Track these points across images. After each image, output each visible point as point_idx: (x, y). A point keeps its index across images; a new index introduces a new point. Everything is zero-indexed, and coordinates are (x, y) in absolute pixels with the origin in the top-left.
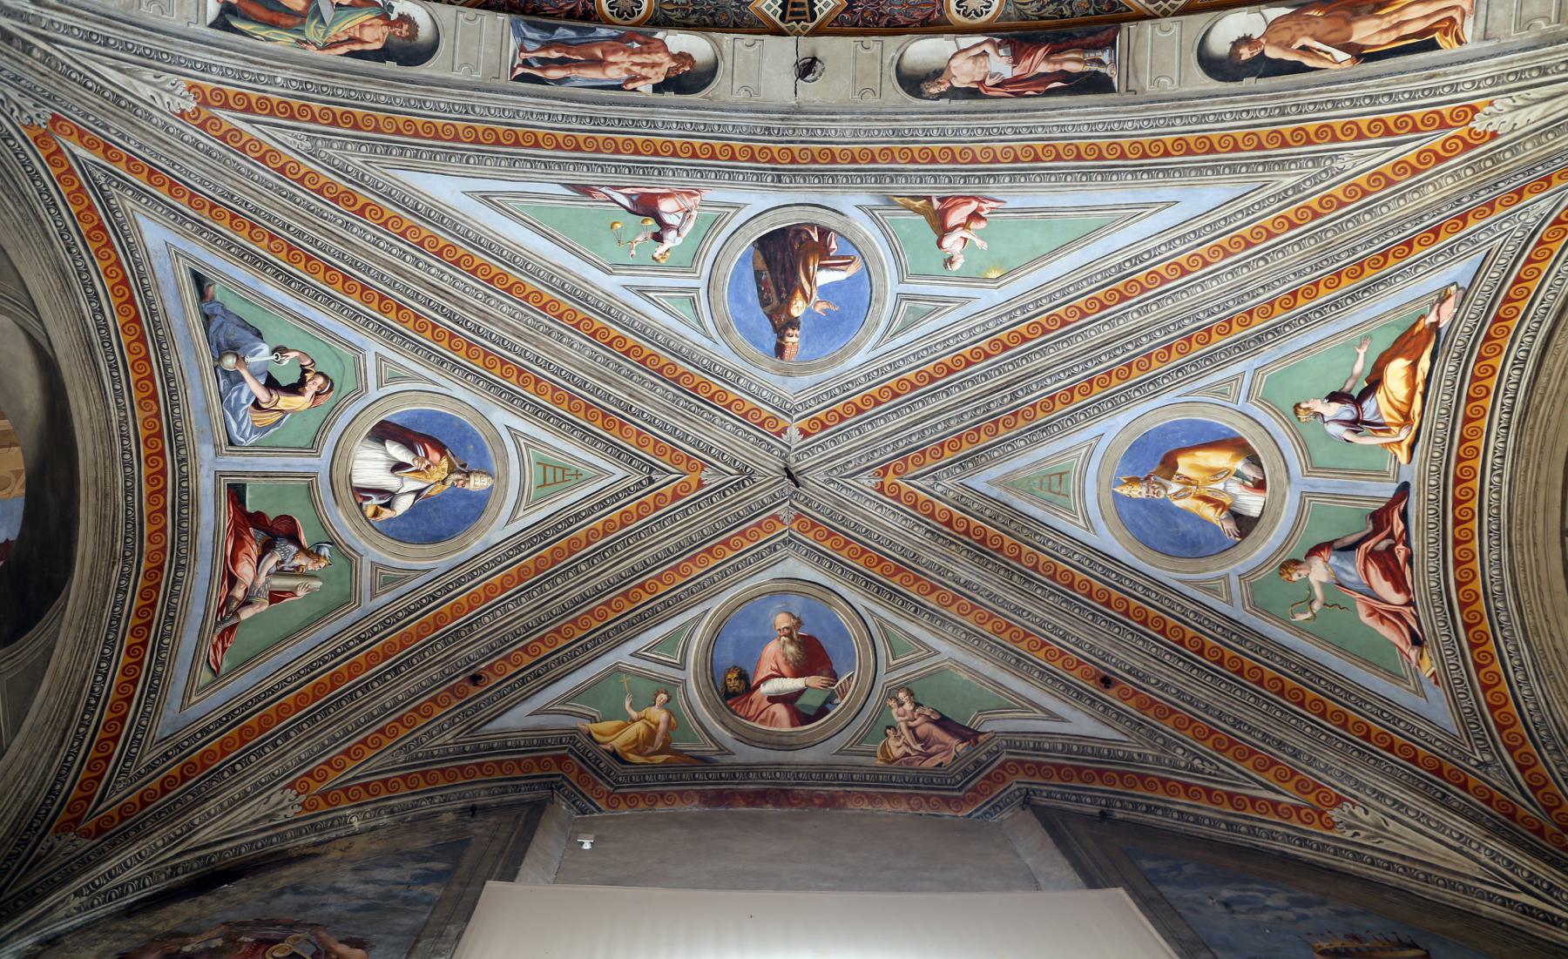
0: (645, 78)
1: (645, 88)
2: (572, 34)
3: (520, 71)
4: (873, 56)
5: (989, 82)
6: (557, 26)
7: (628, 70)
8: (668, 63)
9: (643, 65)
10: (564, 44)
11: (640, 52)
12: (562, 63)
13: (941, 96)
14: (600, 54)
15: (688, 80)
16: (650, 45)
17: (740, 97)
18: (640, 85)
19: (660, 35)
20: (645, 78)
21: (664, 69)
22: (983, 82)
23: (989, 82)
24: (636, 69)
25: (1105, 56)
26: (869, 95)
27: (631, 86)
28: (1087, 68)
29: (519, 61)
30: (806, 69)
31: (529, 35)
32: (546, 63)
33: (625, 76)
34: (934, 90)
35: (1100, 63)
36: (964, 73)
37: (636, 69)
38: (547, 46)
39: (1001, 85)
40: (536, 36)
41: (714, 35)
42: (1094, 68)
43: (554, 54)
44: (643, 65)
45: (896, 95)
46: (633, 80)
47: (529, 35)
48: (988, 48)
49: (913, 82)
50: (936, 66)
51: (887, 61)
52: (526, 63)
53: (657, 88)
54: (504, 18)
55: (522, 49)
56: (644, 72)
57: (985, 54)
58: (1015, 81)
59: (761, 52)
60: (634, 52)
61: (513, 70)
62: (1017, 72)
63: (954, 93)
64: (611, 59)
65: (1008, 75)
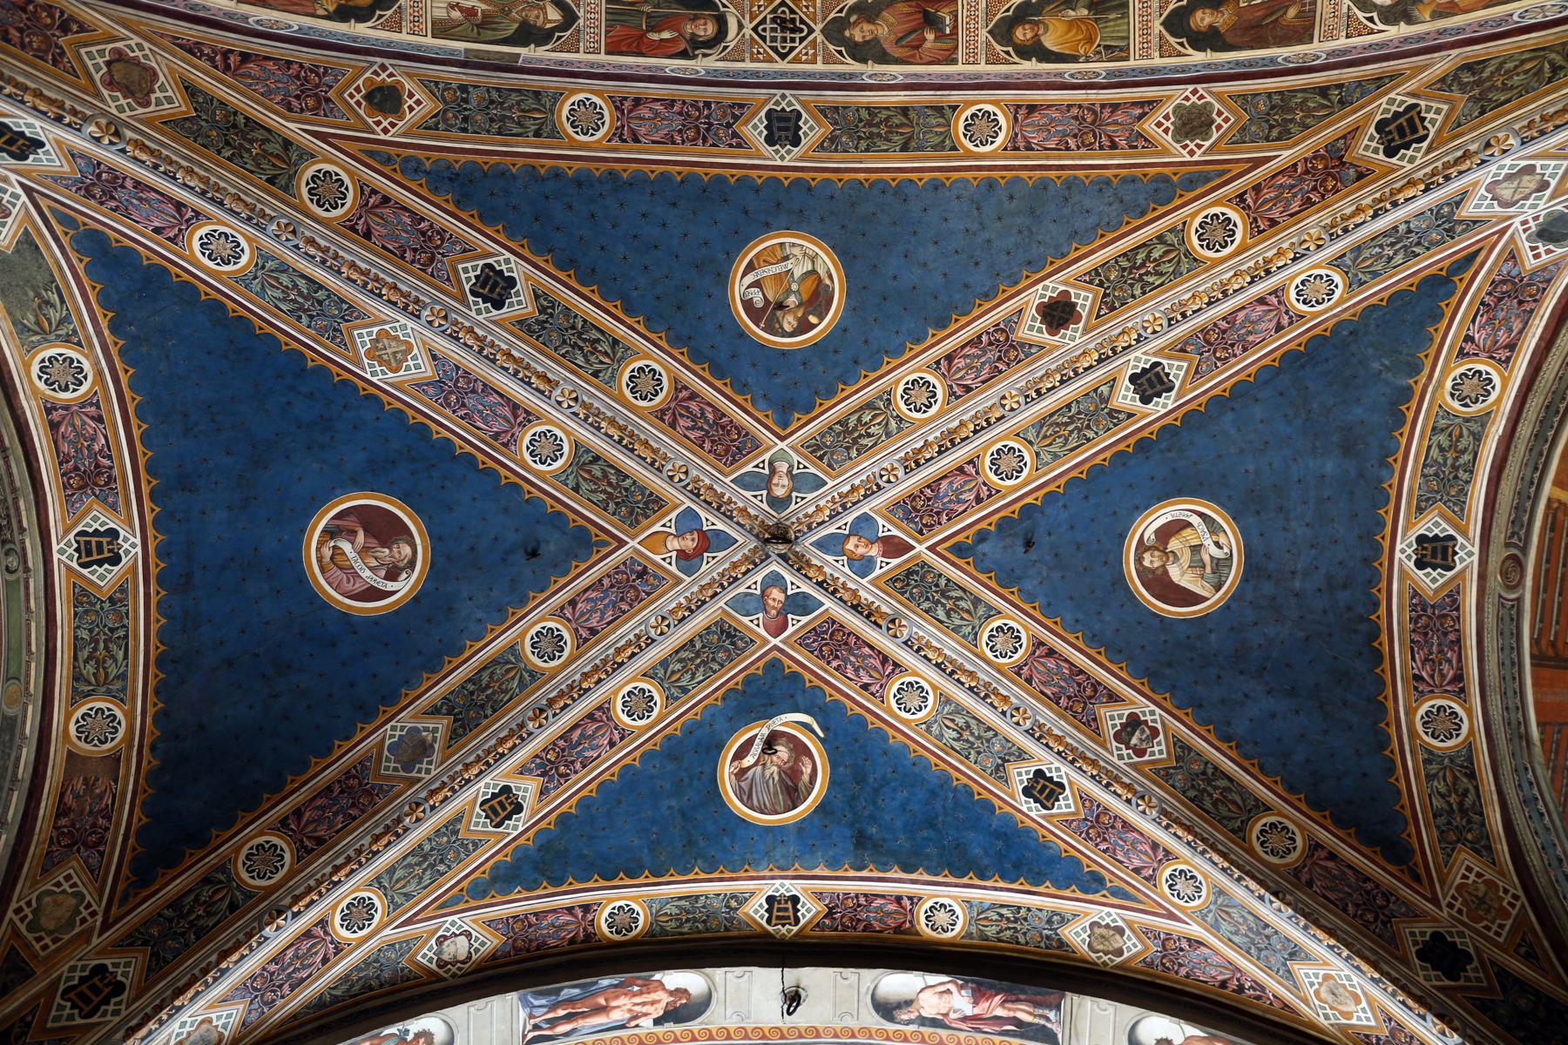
0: (646, 1015)
1: (647, 1023)
2: (577, 991)
3: (530, 1035)
4: (850, 986)
5: (952, 1016)
6: (562, 989)
7: (630, 1011)
8: (666, 999)
9: (644, 1004)
10: (570, 1001)
11: (641, 993)
12: (569, 1018)
13: (909, 1022)
14: (602, 1001)
15: (683, 1010)
16: (648, 987)
17: (732, 1023)
18: (643, 1022)
19: (658, 976)
20: (646, 1015)
21: (663, 1004)
22: (946, 1015)
23: (952, 1016)
24: (637, 1008)
25: (1052, 1015)
26: (848, 1017)
27: (633, 1023)
28: (1036, 1021)
29: (529, 1027)
30: (793, 999)
31: (536, 1003)
32: (553, 1022)
33: (628, 1016)
34: (905, 1017)
35: (1048, 1019)
36: (930, 1005)
37: (637, 1008)
38: (553, 1007)
39: (965, 1019)
40: (543, 1002)
41: (708, 970)
42: (1042, 1022)
43: (561, 1013)
44: (644, 1004)
45: (873, 1020)
46: (635, 1018)
47: (536, 1003)
48: (952, 987)
49: (886, 1009)
50: (908, 997)
51: (863, 990)
52: (536, 1027)
53: (657, 1022)
54: (512, 997)
55: (531, 1016)
56: (644, 1009)
57: (948, 992)
58: (975, 1018)
59: (750, 982)
60: (635, 995)
61: (524, 1036)
62: (977, 1011)
63: (923, 1021)
64: (614, 1004)
65: (969, 1013)
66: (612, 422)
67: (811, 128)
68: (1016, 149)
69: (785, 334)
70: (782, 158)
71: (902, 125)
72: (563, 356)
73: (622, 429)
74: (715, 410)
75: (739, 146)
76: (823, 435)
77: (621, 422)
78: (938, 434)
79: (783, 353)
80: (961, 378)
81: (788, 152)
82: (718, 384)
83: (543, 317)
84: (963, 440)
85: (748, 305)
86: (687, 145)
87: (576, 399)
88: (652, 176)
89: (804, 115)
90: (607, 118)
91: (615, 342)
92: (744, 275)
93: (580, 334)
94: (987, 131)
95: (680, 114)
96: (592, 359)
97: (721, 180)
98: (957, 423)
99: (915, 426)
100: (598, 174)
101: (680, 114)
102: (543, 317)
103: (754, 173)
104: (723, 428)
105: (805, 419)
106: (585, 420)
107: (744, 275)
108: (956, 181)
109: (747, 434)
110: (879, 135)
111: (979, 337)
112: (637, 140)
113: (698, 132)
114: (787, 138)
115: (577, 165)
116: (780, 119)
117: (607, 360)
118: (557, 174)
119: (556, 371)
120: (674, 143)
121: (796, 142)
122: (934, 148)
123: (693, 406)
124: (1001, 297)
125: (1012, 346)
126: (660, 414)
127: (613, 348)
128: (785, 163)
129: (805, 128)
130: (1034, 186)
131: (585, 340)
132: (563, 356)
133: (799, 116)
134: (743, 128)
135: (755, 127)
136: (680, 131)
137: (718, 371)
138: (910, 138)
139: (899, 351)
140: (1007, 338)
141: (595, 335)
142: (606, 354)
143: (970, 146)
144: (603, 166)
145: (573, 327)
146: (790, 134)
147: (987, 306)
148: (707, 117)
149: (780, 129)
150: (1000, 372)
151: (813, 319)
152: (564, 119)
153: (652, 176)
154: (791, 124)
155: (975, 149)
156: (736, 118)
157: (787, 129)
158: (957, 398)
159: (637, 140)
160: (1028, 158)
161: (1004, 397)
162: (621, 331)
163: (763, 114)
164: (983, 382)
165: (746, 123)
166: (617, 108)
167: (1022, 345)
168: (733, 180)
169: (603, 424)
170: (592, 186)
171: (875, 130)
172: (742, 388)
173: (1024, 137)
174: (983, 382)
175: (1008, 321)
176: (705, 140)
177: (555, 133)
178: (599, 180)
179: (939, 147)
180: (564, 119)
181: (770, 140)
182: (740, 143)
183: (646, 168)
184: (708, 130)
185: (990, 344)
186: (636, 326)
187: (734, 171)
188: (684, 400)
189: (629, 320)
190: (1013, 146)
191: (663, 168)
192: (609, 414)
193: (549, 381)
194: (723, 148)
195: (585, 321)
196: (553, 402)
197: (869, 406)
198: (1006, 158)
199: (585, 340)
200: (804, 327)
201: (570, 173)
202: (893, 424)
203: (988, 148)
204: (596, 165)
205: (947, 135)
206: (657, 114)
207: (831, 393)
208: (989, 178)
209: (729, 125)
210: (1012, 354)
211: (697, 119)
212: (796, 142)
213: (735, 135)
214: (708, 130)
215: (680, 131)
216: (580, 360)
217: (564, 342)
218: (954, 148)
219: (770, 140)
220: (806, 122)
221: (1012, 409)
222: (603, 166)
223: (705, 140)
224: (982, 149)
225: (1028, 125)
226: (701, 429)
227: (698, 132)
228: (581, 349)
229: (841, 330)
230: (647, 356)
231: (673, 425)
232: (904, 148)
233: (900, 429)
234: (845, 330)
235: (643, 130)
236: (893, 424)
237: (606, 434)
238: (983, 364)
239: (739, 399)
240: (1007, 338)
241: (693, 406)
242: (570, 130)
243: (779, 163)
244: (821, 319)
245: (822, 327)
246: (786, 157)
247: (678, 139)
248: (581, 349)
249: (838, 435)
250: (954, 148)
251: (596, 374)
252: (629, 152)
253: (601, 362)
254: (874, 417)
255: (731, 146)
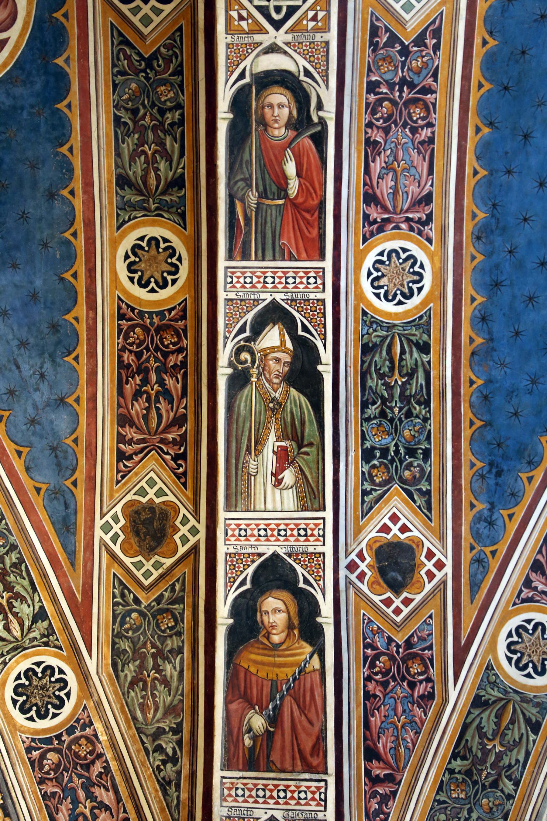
75: (437, 33)
86: (435, 118)
88: (483, 173)
90: (396, 244)
95: (386, 131)
97: (490, 63)
100: (480, 257)
101: (386, 131)
112: (428, 199)
113: (414, 101)
115: (467, 289)
118: (483, 319)
120: (431, 140)
134: (410, 27)
136: (414, 131)
144: (468, 249)
148: (391, 86)
152: (400, 309)
153: (483, 173)
156: (393, 39)
159: (428, 199)
165: (402, 23)
166: (381, 230)
168: (492, 43)
170: (497, 266)
178: (488, 255)
180: (400, 309)
183: (469, 183)
184: (412, 86)
187: (477, 41)
191: (470, 157)
201: (480, 299)
204: (466, 259)
206: (388, 168)
209: (405, 52)
211: (393, 102)
213: (420, 41)
214: (412, 86)
215: (414, 131)
222: (468, 249)
227: (414, 101)
235: (413, 189)
242: (416, 300)
247: (425, 133)
252: (445, 208)
255: (436, 47)
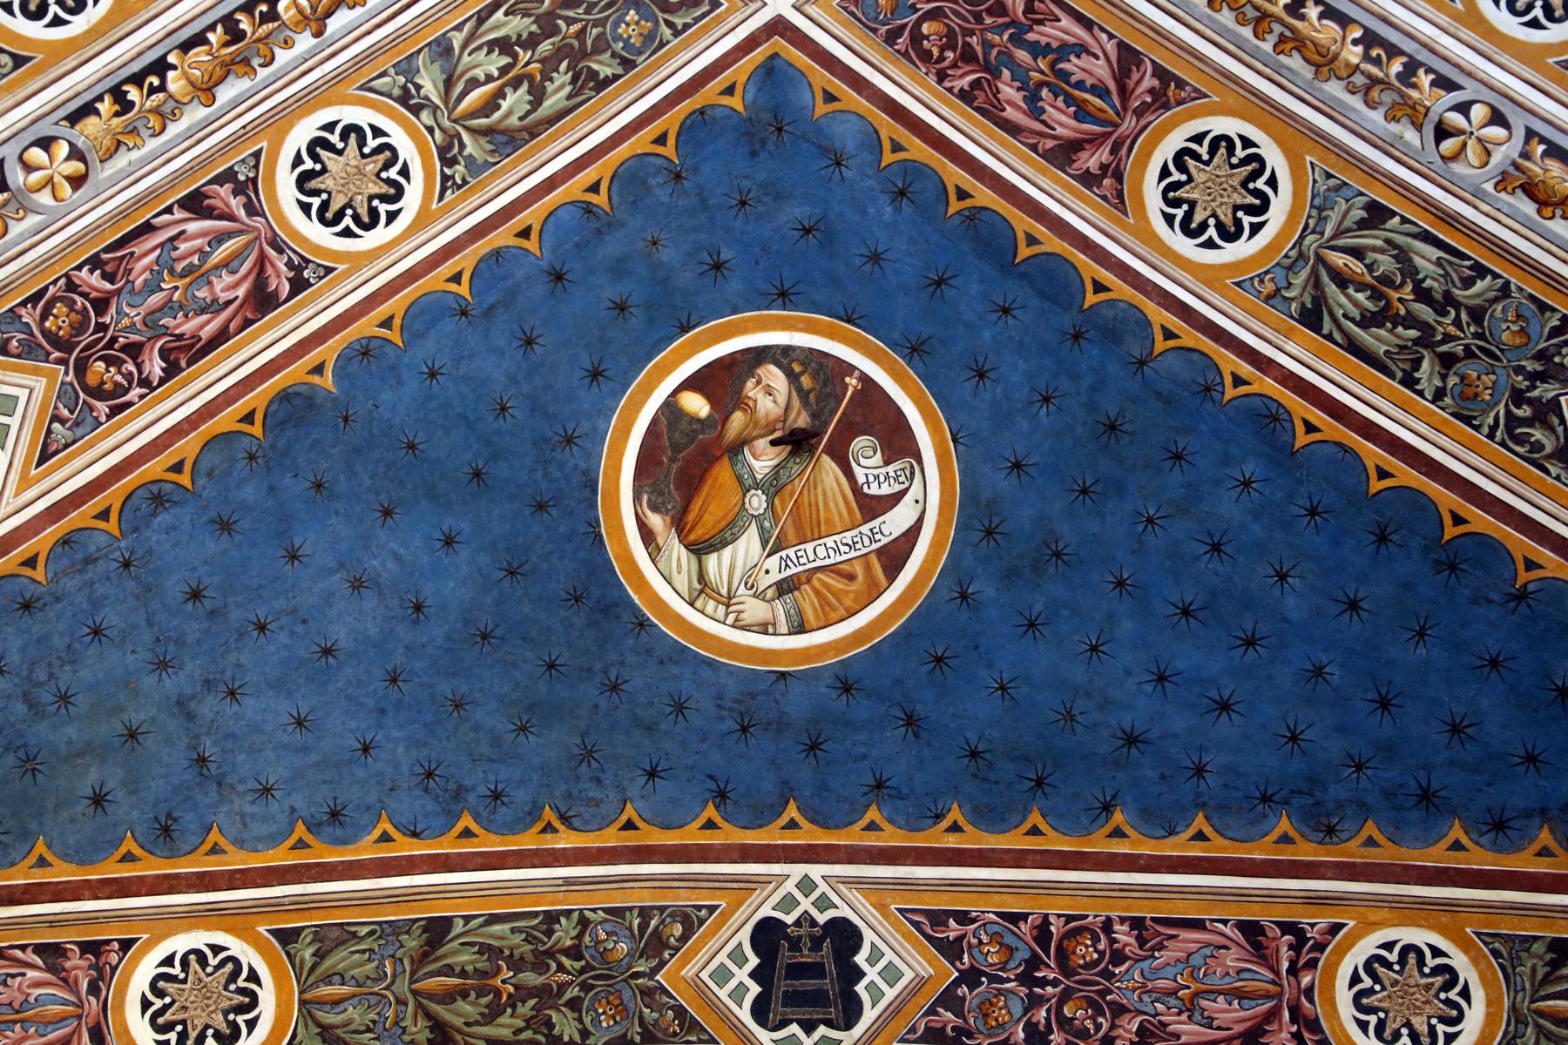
66: (1324, 62)
67: (722, 975)
68: (89, 948)
69: (781, 356)
70: (806, 885)
71: (448, 997)
72: (1481, 271)
73: (1293, 42)
74: (992, 113)
75: (938, 918)
76: (652, 42)
77: (1295, 62)
78: (283, 57)
79: (784, 297)
80: (219, 238)
81: (788, 903)
82: (984, 196)
83: (1545, 391)
84: (199, 40)
85: (898, 443)
86: (1094, 917)
87: (1442, 132)
88: (1200, 822)
89: (745, 1015)
90: (1344, 997)
91: (1311, 317)
92: (913, 533)
93: (1427, 337)
94: (187, 993)
95: (1119, 1010)
96: (1386, 263)
97: (991, 816)
98: (225, 94)
99: (354, 81)
100: (1370, 829)
101: (1119, 1010)
102: (1545, 391)
103: (892, 837)
104: (968, 56)
105: (710, 93)
106: (1412, 67)
107: (913, 533)
108: (274, 840)
109: (891, 38)
110: (517, 964)
111: (171, 371)
112: (1251, 930)
113: (1063, 956)
114: (795, 944)
115: (1434, 856)
116: (818, 999)
117: (1339, 260)
118: (1499, 828)
119: (1508, 223)
120: (1137, 924)
121: (767, 935)
122: (346, 935)
123: (1063, 123)
124: (113, 495)
125: (65, 346)
126: (1170, 92)
127: (1320, 300)
128: (797, 870)
129: (742, 975)
130: (27, 837)
131: (1410, 321)
132: (1481, 271)
133: (760, 1011)
134: (926, 970)
135: (891, 975)
136: (1118, 957)
137: (987, 236)
138: (424, 957)
139: (423, 317)
140: (81, 369)
141: (1378, 340)
142: (1342, 280)
143: (237, 947)
144: (1352, 851)
145: (1447, 361)
146: (785, 956)
147: (154, 467)
148: (1034, 1002)
149: (817, 970)
150: (95, 263)
151: (696, 404)
152: (1478, 994)
153: (1200, 822)
154: (782, 985)
155: (220, 938)
156: (948, 999)
157: (796, 971)
158: (228, 176)
159: (1251, 930)
160: (53, 922)
161: (77, 182)
162: (1295, 354)
163: (869, 1015)
164: (148, 228)
165: (919, 985)
166: (1314, 1025)
167: (30, 350)
168: (955, 815)
169: (1353, 54)
170: (1388, 795)
171: (530, 978)
172: (909, 185)
173: (68, 983)
174: (148, 228)
175: (83, 423)
176: (1042, 933)
177: (1506, 952)
178: (1365, 811)
179: (330, 940)
180: (1478, 994)
181: (844, 936)
182: (936, 926)
183: (1220, 848)
184: (1034, 963)
185: (134, 350)
186: (1246, 369)
187: (952, 841)
188: (1095, 141)
189: (1270, 386)
190: (103, 956)
191: (1170, 848)
192: (1334, 88)
193: (1530, 189)
194: (987, 908)
195: (1409, 382)
196: (1519, 122)
197: (507, 141)
198: (122, 917)
199: (1410, 321)
200: (722, 382)
201: (1457, 832)
202: (429, 84)
203: (180, 943)
204: (1374, 856)
205: (309, 977)
206: (1190, 1008)
207: (631, 178)
208: (173, 854)
209: (971, 977)
210: (60, 320)
211: (1065, 997)
212: (767, 935)
213: (951, 949)
214: (1034, 963)
215: (1118, 957)
216: (1425, 258)
217: (1477, 315)
218: (286, 937)
219: (844, 936)
220: (739, 993)
221: (46, 143)
222: (1352, 851)
223: (1042, 933)
224: (198, 939)
225: (61, 1020)
226: (1037, 50)
227: (1063, 956)
228: (1423, 295)
229: (608, 376)
230: (1210, 276)
231: (1128, 58)
232: (438, 930)
233: (407, 68)
234: (595, 374)
235: (1231, 959)
236: (429, 84)
237: (1344, 21)
238: (153, 287)
239: (918, 150)
240: (81, 369)
241: (1063, 123)
242: (1459, 960)
243: (816, 871)
244: (670, 407)
245: (667, 382)
246: (796, 889)
247: (1123, 935)
248: (1423, 295)
249: (601, 45)
250: (286, 937)
251: (1377, 214)
252: (1271, 896)
253: (1357, 253)
254: (491, 105)
255: (963, 918)
